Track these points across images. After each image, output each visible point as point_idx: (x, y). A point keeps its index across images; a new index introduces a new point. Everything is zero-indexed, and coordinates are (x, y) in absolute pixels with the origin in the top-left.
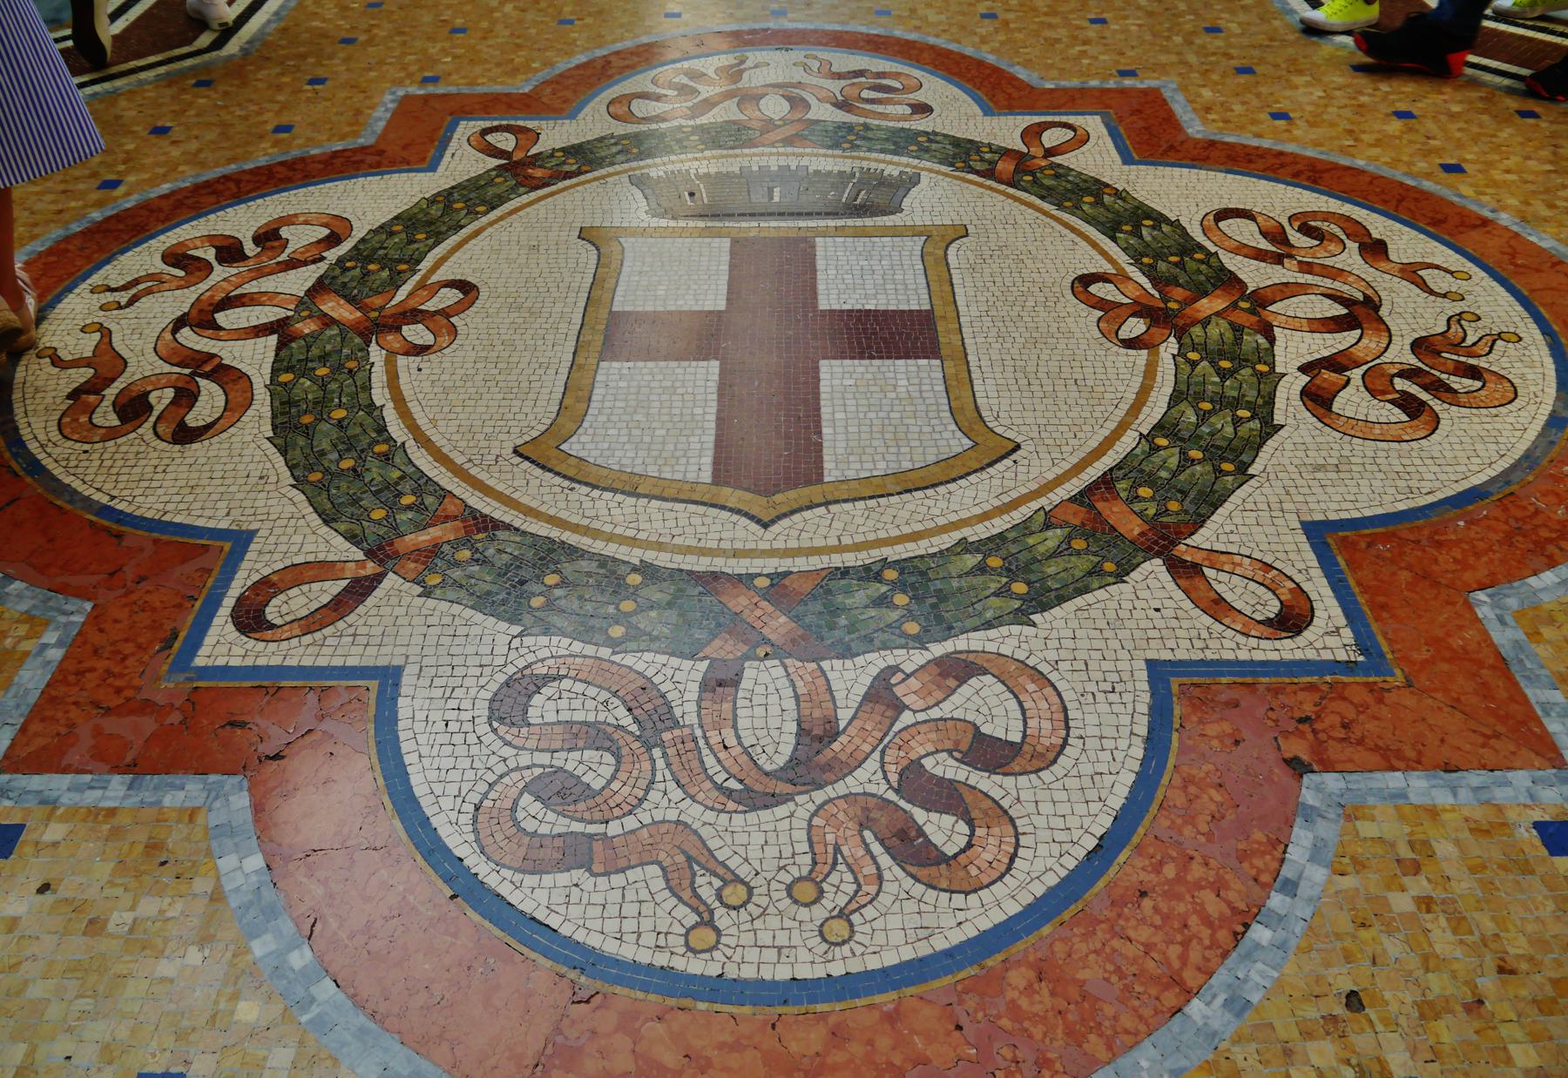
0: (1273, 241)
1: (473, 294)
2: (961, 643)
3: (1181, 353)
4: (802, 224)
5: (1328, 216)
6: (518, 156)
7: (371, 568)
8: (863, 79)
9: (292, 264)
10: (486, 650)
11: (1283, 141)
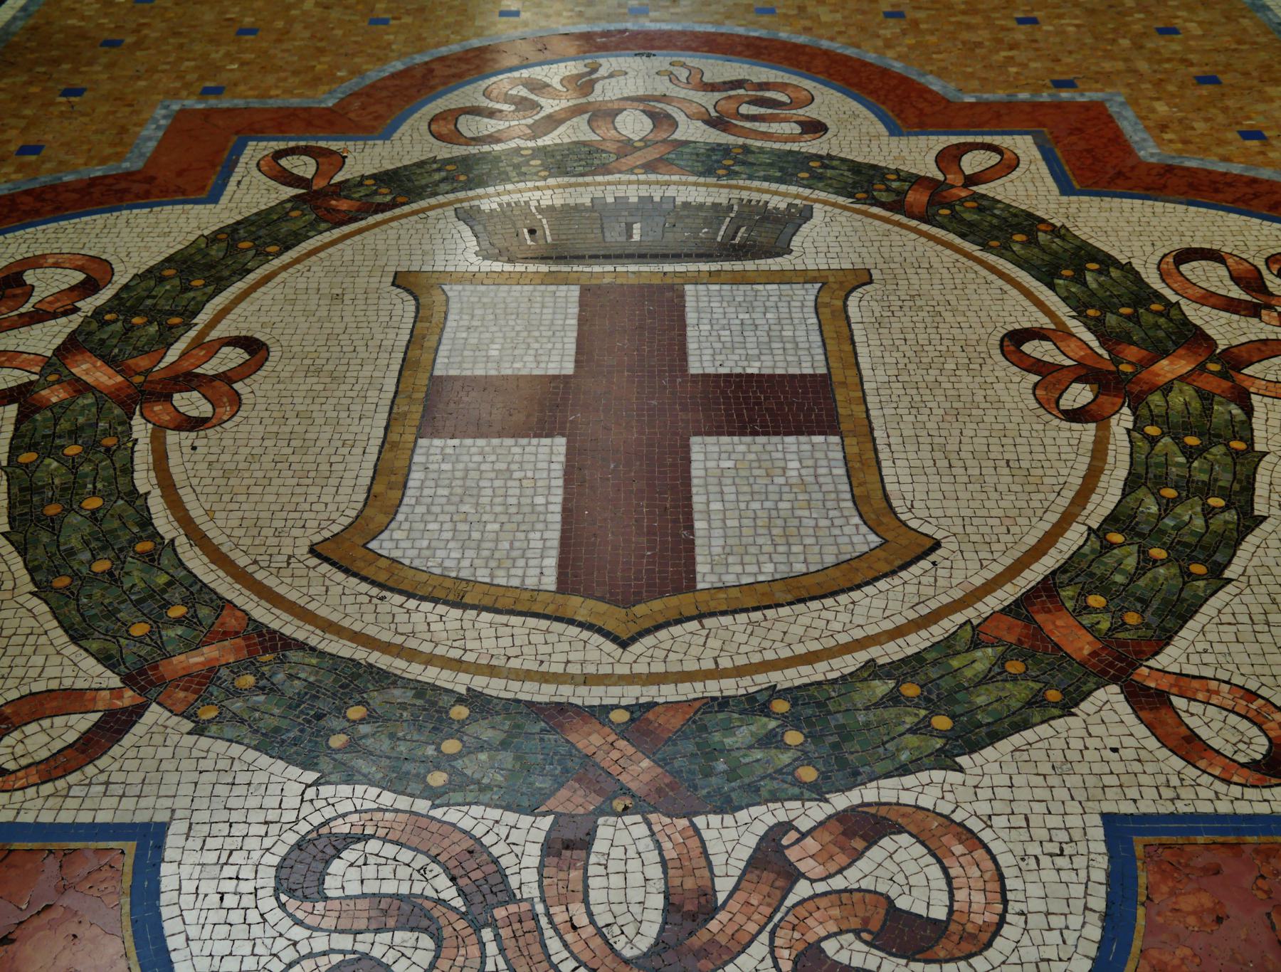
1: (262, 353)
2: (869, 793)
3: (1137, 427)
4: (668, 268)
6: (319, 184)
7: (129, 697)
8: (741, 92)
9: (38, 316)
10: (272, 802)
11: (1257, 166)
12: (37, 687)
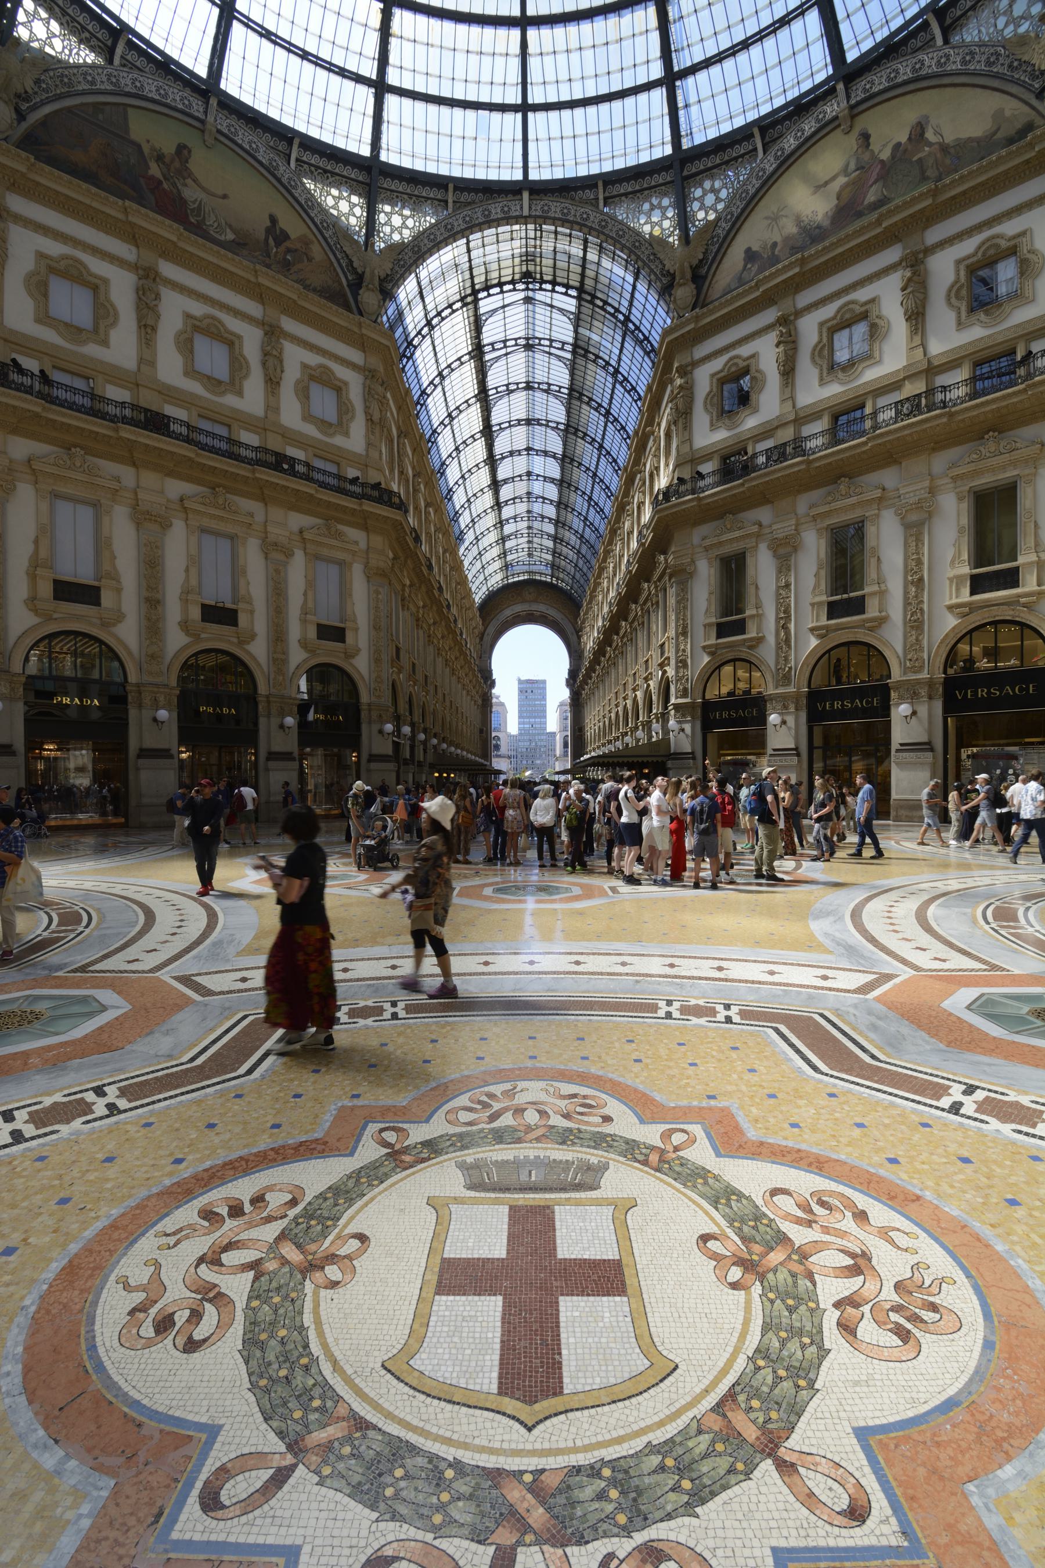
0: (804, 1211)
4: (547, 1196)
5: (832, 1193)
6: (397, 1147)
7: (289, 1460)
9: (269, 1219)
10: (354, 1533)
12: (246, 1451)
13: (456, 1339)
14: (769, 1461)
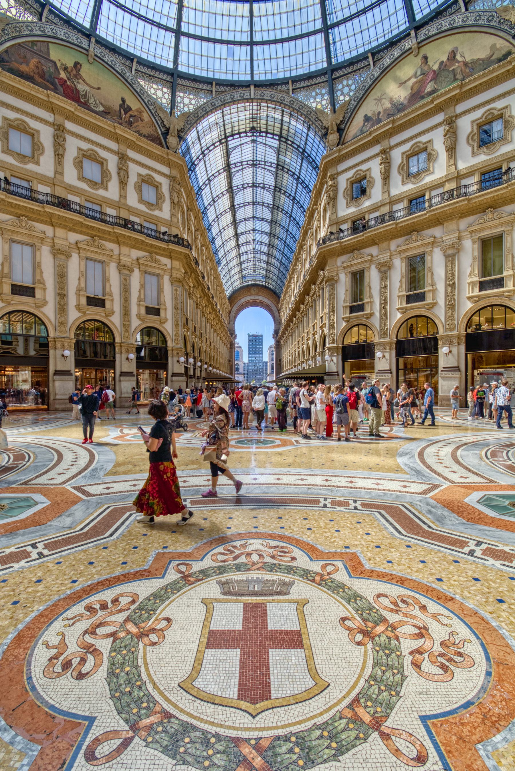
0: (394, 605)
4: (263, 598)
5: (408, 596)
6: (187, 573)
7: (131, 734)
9: (121, 611)
13: (216, 671)
14: (376, 733)
